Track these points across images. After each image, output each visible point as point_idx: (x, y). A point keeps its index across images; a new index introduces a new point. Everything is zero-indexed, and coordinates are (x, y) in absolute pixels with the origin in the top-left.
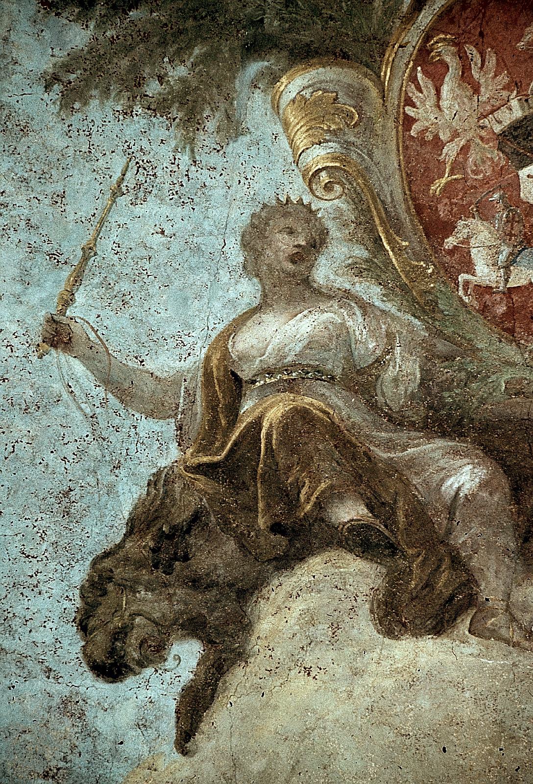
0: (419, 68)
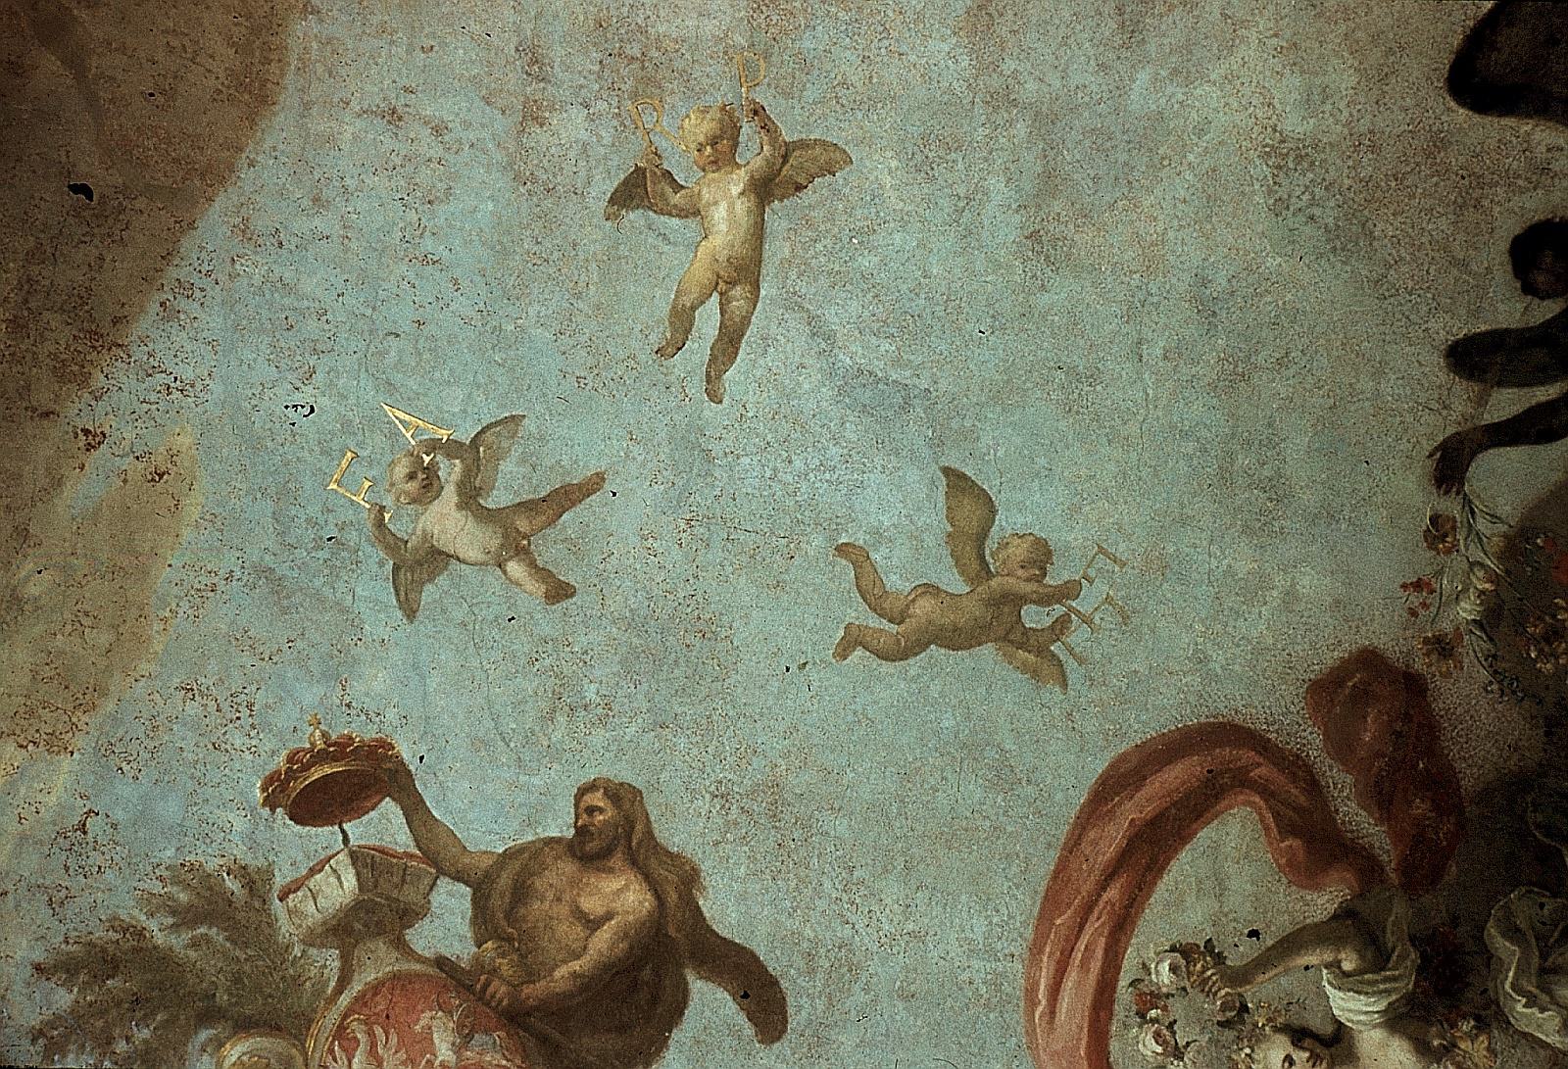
0: (337, 1043)
